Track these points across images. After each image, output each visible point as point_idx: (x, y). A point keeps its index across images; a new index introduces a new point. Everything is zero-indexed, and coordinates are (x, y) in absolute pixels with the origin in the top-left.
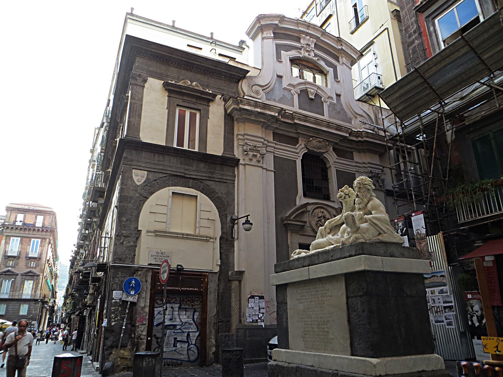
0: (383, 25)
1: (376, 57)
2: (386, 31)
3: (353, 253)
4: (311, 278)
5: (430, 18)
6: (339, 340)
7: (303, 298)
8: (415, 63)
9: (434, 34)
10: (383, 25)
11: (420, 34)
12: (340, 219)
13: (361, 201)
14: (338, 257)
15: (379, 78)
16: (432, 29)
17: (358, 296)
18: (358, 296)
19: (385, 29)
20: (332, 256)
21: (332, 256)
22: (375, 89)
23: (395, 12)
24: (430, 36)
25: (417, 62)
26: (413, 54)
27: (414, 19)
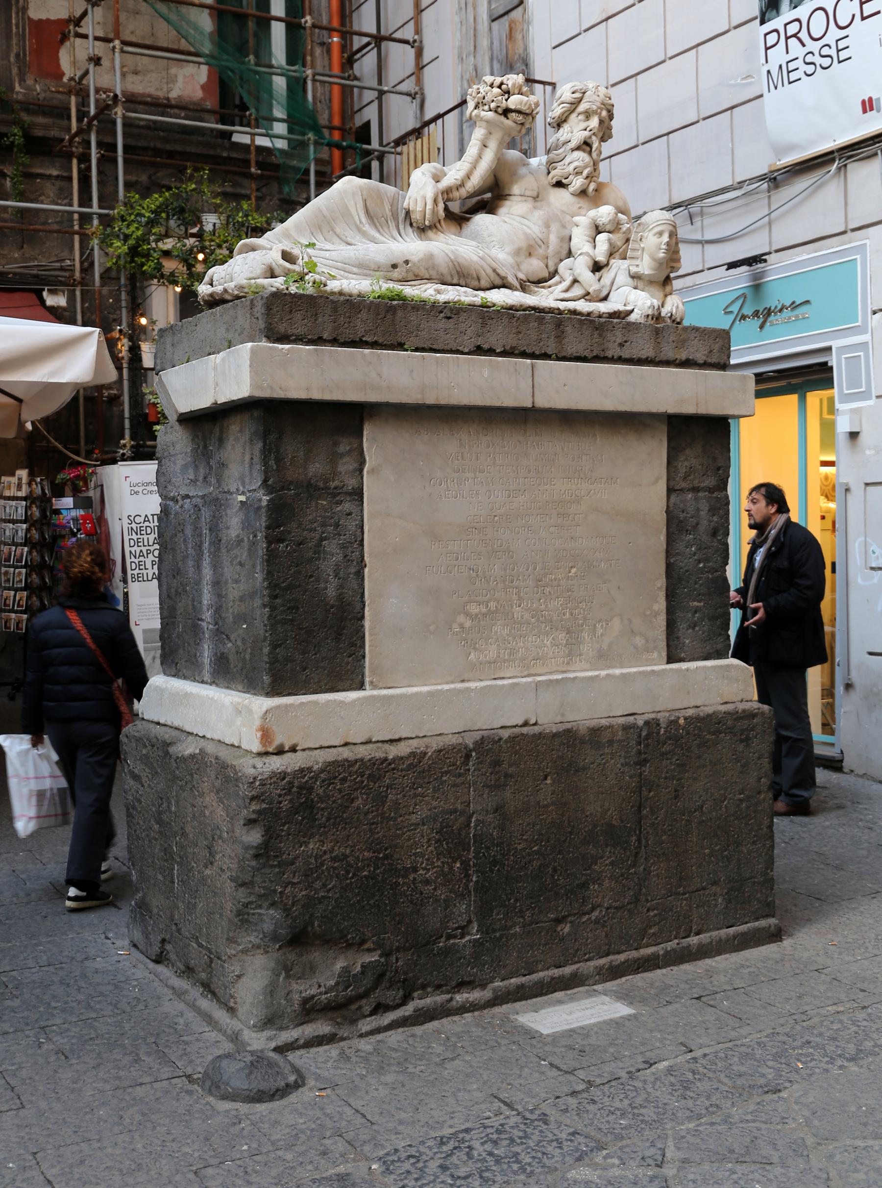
3: (700, 358)
4: (542, 402)
6: (630, 621)
7: (471, 475)
14: (644, 354)
17: (704, 489)
18: (704, 489)
20: (621, 345)
21: (621, 345)
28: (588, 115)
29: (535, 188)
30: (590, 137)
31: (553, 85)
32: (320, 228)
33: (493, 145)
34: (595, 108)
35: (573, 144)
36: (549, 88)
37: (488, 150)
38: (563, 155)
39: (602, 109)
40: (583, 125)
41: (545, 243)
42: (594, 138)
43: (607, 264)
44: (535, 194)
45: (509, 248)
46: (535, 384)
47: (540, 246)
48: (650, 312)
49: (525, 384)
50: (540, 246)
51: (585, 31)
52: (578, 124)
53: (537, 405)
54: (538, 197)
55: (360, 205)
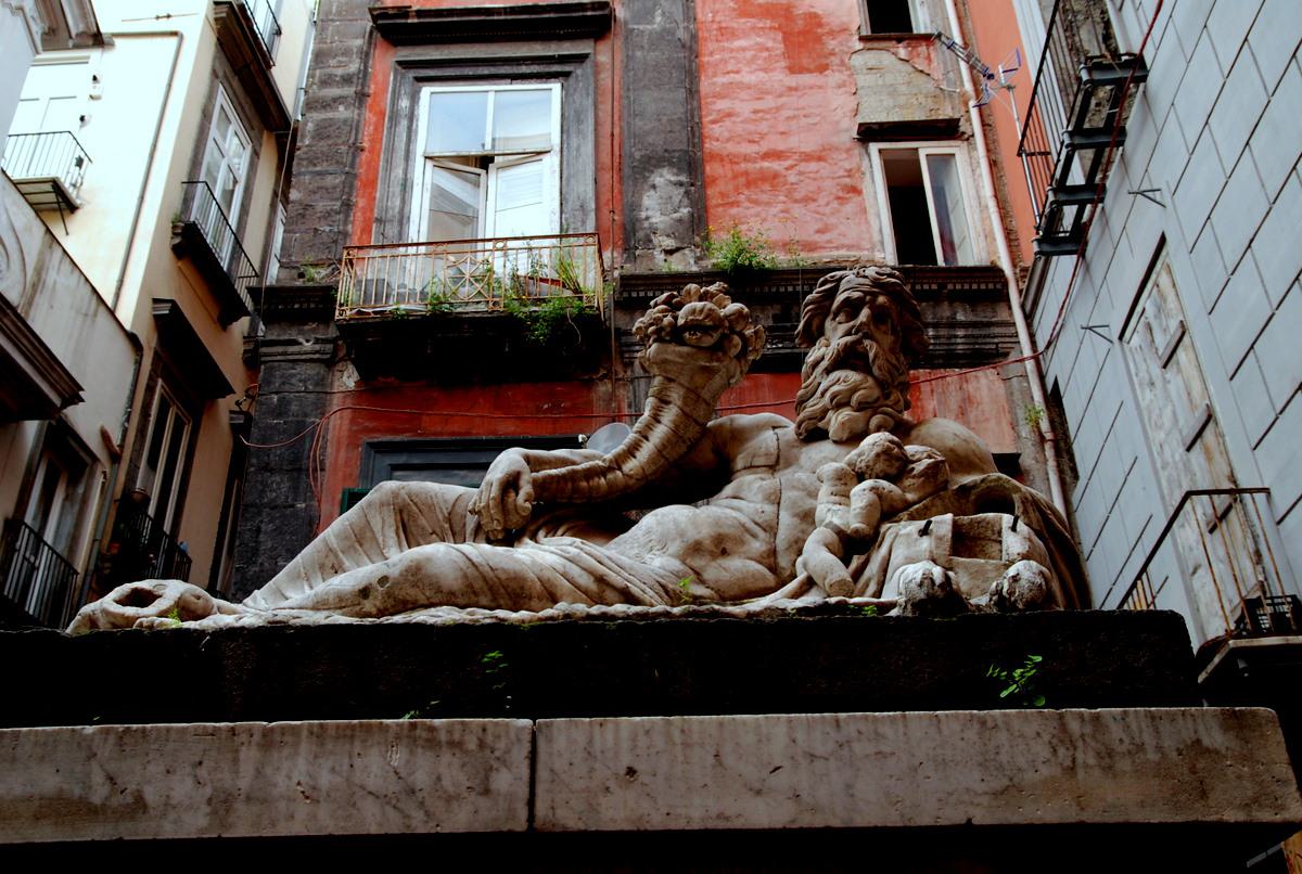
0: (169, 16)
1: (95, 93)
2: (174, 41)
5: (412, 74)
8: (311, 169)
9: (404, 123)
10: (169, 16)
11: (362, 96)
12: (610, 469)
13: (876, 393)
15: (80, 163)
16: (404, 103)
19: (175, 34)
22: (48, 187)
23: (225, 8)
24: (391, 118)
25: (318, 169)
26: (313, 138)
27: (359, 42)
28: (852, 308)
29: (773, 450)
30: (859, 342)
31: (1266, 491)
32: (322, 567)
33: (676, 395)
34: (856, 294)
35: (824, 364)
36: (1260, 497)
37: (671, 406)
38: (815, 383)
39: (875, 295)
40: (843, 328)
41: (771, 529)
42: (867, 342)
43: (877, 532)
44: (772, 461)
45: (675, 547)
46: (543, 774)
47: (754, 536)
48: (921, 595)
49: (509, 780)
50: (754, 536)
51: (1281, 412)
52: (835, 329)
53: (538, 824)
54: (777, 462)
55: (391, 520)
